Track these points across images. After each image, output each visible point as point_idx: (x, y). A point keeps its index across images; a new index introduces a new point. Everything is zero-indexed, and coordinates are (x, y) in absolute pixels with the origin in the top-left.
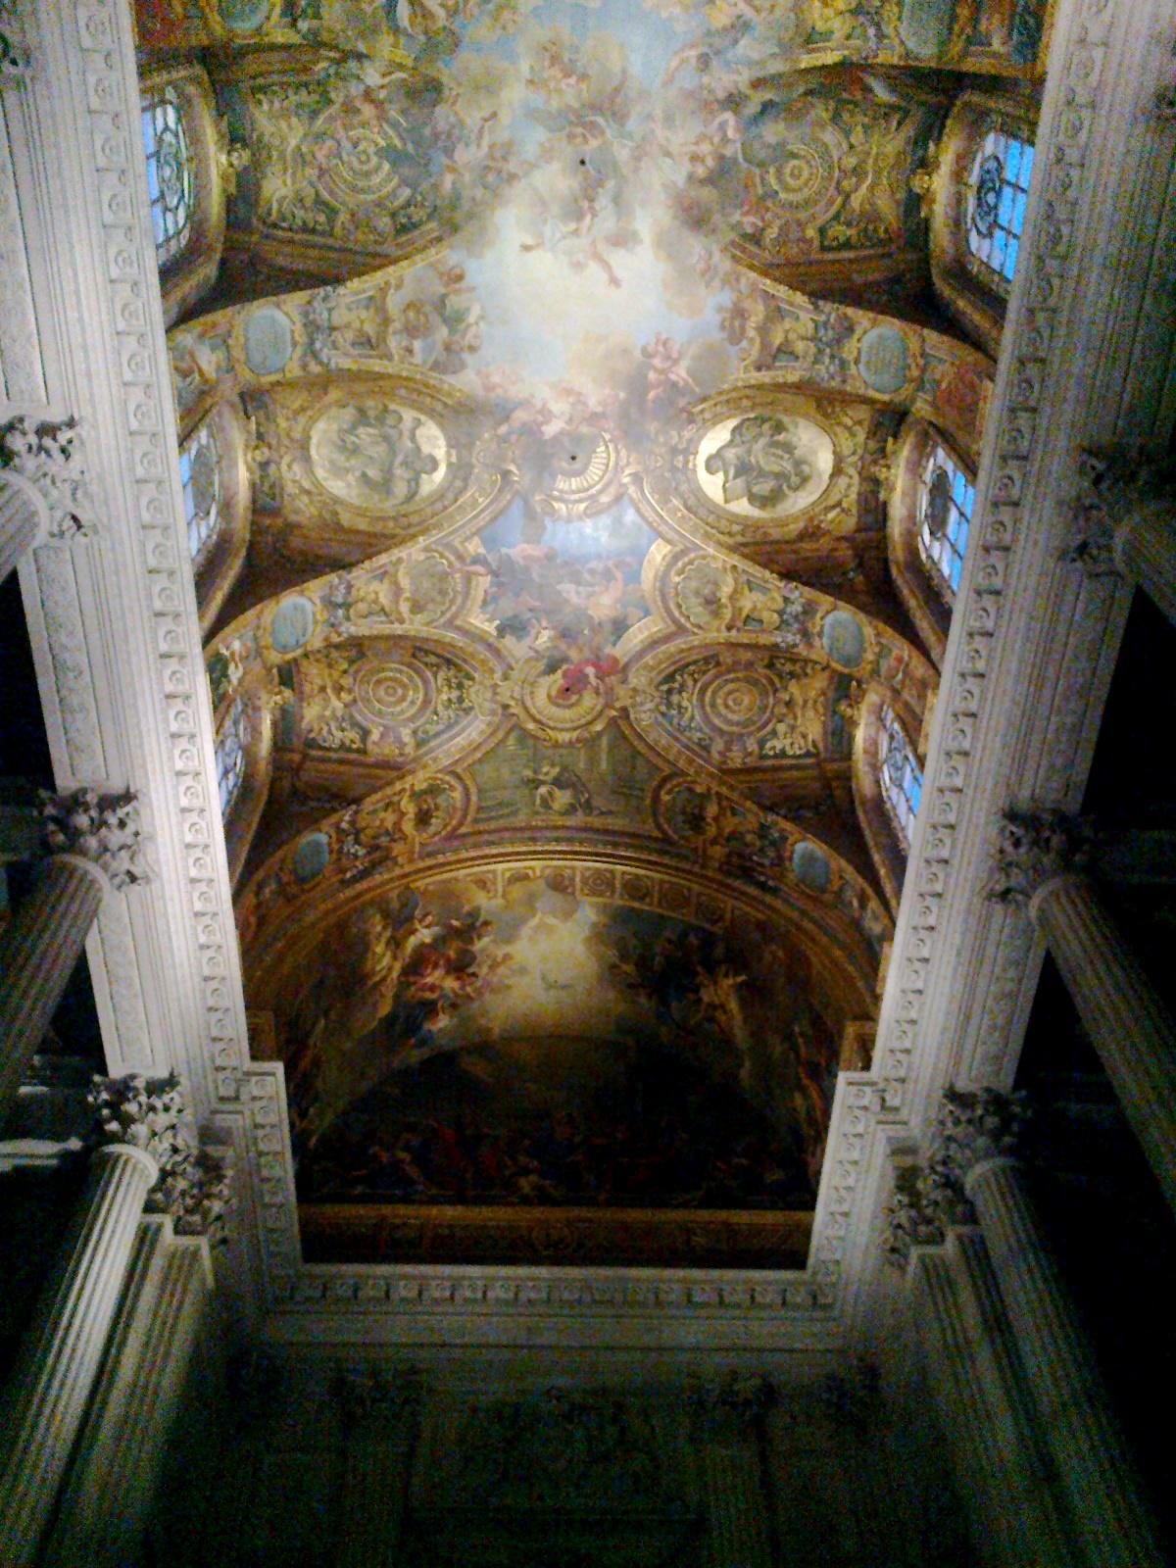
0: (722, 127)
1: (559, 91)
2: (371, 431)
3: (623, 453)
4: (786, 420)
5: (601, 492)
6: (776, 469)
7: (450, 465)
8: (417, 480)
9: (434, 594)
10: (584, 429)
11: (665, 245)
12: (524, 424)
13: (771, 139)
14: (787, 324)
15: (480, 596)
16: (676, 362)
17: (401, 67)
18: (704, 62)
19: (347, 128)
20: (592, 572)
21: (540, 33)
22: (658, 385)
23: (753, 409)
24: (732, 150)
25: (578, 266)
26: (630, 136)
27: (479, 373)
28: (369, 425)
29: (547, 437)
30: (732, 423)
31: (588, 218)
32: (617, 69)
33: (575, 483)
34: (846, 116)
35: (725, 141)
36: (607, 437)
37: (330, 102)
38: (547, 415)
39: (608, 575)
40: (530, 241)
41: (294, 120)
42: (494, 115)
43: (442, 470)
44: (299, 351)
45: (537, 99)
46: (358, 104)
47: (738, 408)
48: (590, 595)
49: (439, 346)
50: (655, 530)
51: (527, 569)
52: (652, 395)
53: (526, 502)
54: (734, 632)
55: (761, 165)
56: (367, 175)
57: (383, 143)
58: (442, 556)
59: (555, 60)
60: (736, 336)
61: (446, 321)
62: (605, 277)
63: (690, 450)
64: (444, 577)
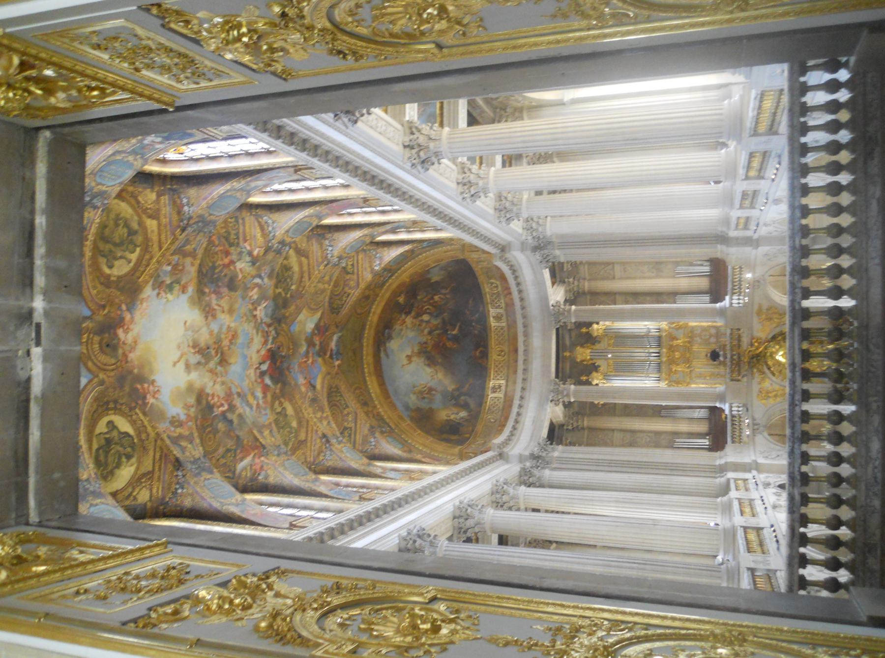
0: (222, 405)
2: (126, 235)
3: (112, 374)
4: (134, 460)
5: (92, 360)
6: (110, 459)
7: (109, 276)
8: (103, 256)
10: (120, 351)
11: (190, 388)
14: (190, 446)
16: (154, 397)
17: (245, 277)
18: (239, 394)
21: (239, 331)
22: (143, 388)
23: (141, 440)
24: (218, 411)
25: (179, 347)
27: (149, 296)
28: (129, 235)
30: (131, 431)
31: (193, 351)
32: (232, 360)
33: (96, 346)
35: (219, 407)
38: (126, 332)
40: (188, 324)
41: (224, 230)
43: (107, 271)
44: (207, 215)
46: (229, 258)
47: (140, 433)
49: (164, 279)
52: (139, 386)
57: (217, 264)
59: (233, 336)
61: (172, 283)
62: (176, 360)
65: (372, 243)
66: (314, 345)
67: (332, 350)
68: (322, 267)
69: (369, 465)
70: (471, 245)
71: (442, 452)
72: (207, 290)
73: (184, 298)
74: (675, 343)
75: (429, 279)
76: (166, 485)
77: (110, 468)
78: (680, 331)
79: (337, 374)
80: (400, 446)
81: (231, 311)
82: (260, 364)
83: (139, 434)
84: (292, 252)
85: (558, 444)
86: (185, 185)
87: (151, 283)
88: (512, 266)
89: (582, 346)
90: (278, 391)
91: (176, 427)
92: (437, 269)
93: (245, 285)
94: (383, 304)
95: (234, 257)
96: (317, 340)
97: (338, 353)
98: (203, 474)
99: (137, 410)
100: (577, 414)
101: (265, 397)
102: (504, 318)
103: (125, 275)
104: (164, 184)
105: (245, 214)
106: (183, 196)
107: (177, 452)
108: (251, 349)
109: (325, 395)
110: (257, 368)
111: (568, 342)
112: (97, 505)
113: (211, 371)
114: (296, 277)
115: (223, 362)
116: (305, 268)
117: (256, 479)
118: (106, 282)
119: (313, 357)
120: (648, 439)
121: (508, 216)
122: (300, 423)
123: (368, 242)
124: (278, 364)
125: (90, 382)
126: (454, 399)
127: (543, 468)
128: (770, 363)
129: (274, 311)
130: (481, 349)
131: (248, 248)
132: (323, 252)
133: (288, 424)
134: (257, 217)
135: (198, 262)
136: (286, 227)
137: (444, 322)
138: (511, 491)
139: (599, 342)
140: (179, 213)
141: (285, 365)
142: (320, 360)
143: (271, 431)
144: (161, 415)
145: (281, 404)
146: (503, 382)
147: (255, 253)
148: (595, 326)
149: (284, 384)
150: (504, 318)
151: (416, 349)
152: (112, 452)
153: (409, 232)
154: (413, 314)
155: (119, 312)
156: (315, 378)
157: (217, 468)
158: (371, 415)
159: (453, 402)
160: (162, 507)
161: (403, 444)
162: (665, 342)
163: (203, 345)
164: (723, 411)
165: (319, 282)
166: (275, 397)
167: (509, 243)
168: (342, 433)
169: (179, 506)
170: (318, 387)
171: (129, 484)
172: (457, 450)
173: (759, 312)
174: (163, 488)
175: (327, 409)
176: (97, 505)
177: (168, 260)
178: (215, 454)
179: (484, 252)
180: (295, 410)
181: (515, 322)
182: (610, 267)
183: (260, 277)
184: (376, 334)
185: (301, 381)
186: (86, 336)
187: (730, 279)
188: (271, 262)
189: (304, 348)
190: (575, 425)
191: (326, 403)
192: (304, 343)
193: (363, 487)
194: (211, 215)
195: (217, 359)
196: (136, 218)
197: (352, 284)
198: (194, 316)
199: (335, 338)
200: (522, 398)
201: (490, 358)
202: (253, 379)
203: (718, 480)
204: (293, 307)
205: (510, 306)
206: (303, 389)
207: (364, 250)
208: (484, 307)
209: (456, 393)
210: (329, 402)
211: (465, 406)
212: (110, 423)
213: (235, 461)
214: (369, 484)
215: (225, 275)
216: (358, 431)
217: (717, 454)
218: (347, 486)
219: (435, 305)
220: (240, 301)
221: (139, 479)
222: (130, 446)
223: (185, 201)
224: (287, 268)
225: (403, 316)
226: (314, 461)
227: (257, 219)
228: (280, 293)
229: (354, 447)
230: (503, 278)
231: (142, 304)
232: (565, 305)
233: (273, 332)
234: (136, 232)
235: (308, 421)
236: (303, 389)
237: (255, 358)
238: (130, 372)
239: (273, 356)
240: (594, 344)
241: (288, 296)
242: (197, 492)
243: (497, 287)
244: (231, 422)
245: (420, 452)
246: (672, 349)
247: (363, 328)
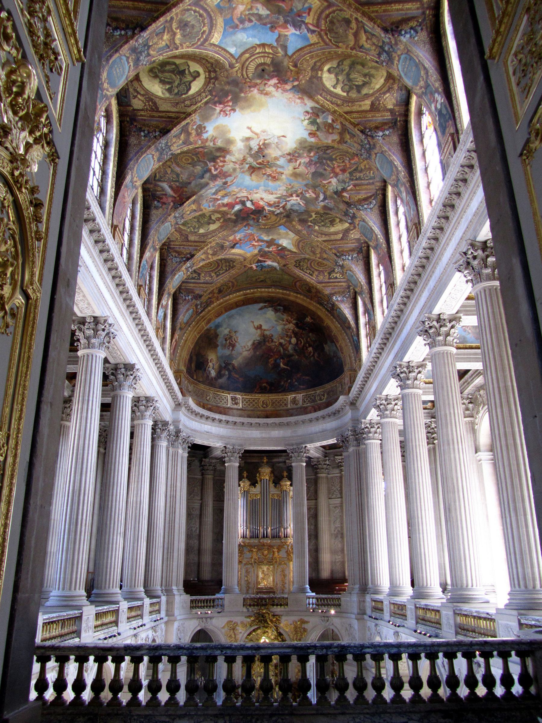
0: (216, 169)
1: (273, 172)
2: (357, 83)
3: (239, 75)
4: (167, 95)
6: (167, 74)
7: (322, 70)
8: (338, 65)
9: (337, 24)
10: (258, 81)
11: (230, 142)
12: (286, 83)
13: (199, 168)
14: (181, 142)
15: (312, 14)
16: (221, 111)
18: (226, 183)
19: (346, 165)
20: (250, 21)
21: (278, 183)
22: (228, 102)
23: (185, 100)
24: (210, 165)
25: (264, 132)
26: (247, 164)
27: (306, 104)
28: (356, 86)
29: (276, 79)
30: (191, 92)
34: (175, 176)
35: (214, 166)
36: (248, 80)
37: (350, 173)
38: (275, 86)
39: (242, 21)
41: (363, 168)
42: (294, 169)
43: (326, 68)
45: (279, 170)
46: (340, 173)
47: (190, 100)
48: (251, 9)
49: (321, 117)
50: (220, 47)
51: (286, 22)
52: (229, 98)
53: (286, 54)
54: (169, 18)
55: (200, 161)
56: (341, 155)
58: (330, 40)
59: (274, 177)
60: (200, 127)
61: (317, 124)
62: (253, 129)
63: (208, 81)
64: (331, 30)
65: (355, 293)
66: (268, 247)
67: (265, 261)
68: (334, 251)
69: (169, 294)
70: (355, 377)
71: (180, 356)
72: (312, 154)
73: (305, 135)
74: (275, 550)
75: (326, 343)
76: (147, 122)
77: (160, 75)
78: (285, 555)
79: (245, 266)
80: (185, 320)
81: (295, 175)
82: (251, 201)
83: (188, 99)
84: (347, 225)
85: (188, 453)
86: (400, 132)
87: (317, 106)
88: (339, 411)
89: (272, 472)
90: (229, 216)
91: (196, 130)
92: (335, 348)
93: (317, 187)
94: (305, 304)
95: (341, 177)
96: (272, 249)
97: (262, 267)
98: (158, 153)
99: (209, 97)
100: (215, 470)
101: (224, 205)
102: (295, 406)
103: (324, 85)
104: (400, 115)
105: (379, 184)
106: (391, 130)
107: (175, 131)
108: (263, 193)
109: (227, 257)
110: (248, 199)
111: (275, 460)
112: (128, 63)
113: (244, 160)
114: (325, 230)
115: (253, 170)
116: (333, 237)
117: (154, 199)
118: (317, 69)
119: (258, 245)
120: (194, 529)
121: (381, 407)
122: (203, 235)
123: (357, 290)
124: (252, 216)
125: (231, 55)
126: (225, 365)
127: (168, 439)
128: (259, 631)
129: (296, 211)
131: (349, 188)
132: (347, 251)
133: (201, 226)
134: (375, 195)
135: (336, 146)
136: (367, 219)
137: (290, 356)
138: (148, 413)
139: (275, 487)
140: (377, 128)
141: (251, 222)
142: (256, 251)
143: (195, 211)
144: (206, 118)
145: (218, 219)
146: (241, 406)
147: (345, 194)
148: (289, 483)
149: (235, 222)
151: (267, 333)
152: (174, 76)
153: (366, 325)
155: (291, 79)
156: (240, 248)
157: (163, 165)
158: (210, 296)
159: (223, 365)
160: (128, 119)
161: (187, 323)
162: (277, 541)
163: (266, 152)
164: (218, 593)
165: (322, 249)
166: (224, 214)
167: (358, 409)
168: (195, 271)
169: (130, 134)
170: (234, 251)
171: (147, 92)
172: (183, 368)
173: (303, 622)
174: (145, 120)
175: (215, 258)
176: (128, 63)
177: (337, 120)
178: (174, 165)
179: (350, 388)
180: (214, 231)
181: (292, 415)
182: (339, 496)
183: (325, 199)
184: (279, 299)
185: (238, 236)
186: (271, 51)
187: (330, 596)
188: (338, 207)
189: (265, 239)
190: (206, 467)
191: (220, 257)
192: (270, 238)
193: (150, 289)
194: (376, 154)
195: (254, 164)
196: (371, 92)
197: (321, 278)
198: (290, 144)
199: (275, 264)
200: (228, 422)
202: (239, 195)
203: (159, 588)
204: (299, 227)
205: (304, 411)
206: (231, 238)
207: (349, 287)
208: (304, 389)
209: (230, 367)
210: (221, 260)
211: (219, 375)
212: (198, 74)
213: (169, 181)
214: (152, 294)
215: (325, 170)
216: (197, 285)
217: (181, 587)
218: (151, 277)
219: (304, 348)
220: (305, 182)
221: (152, 100)
222: (179, 91)
223: (387, 133)
224: (332, 223)
225: (294, 322)
226: (170, 248)
227: (373, 195)
228: (311, 216)
229: (183, 282)
230: (329, 404)
231: (299, 98)
232: (306, 457)
233: (278, 211)
234: (359, 92)
235: (204, 242)
236: (231, 238)
237: (256, 197)
238: (241, 91)
239: (259, 211)
240: (273, 482)
241: (310, 224)
242: (142, 148)
243: (321, 399)
244: (202, 177)
245: (180, 337)
246: (270, 547)
247: (284, 288)
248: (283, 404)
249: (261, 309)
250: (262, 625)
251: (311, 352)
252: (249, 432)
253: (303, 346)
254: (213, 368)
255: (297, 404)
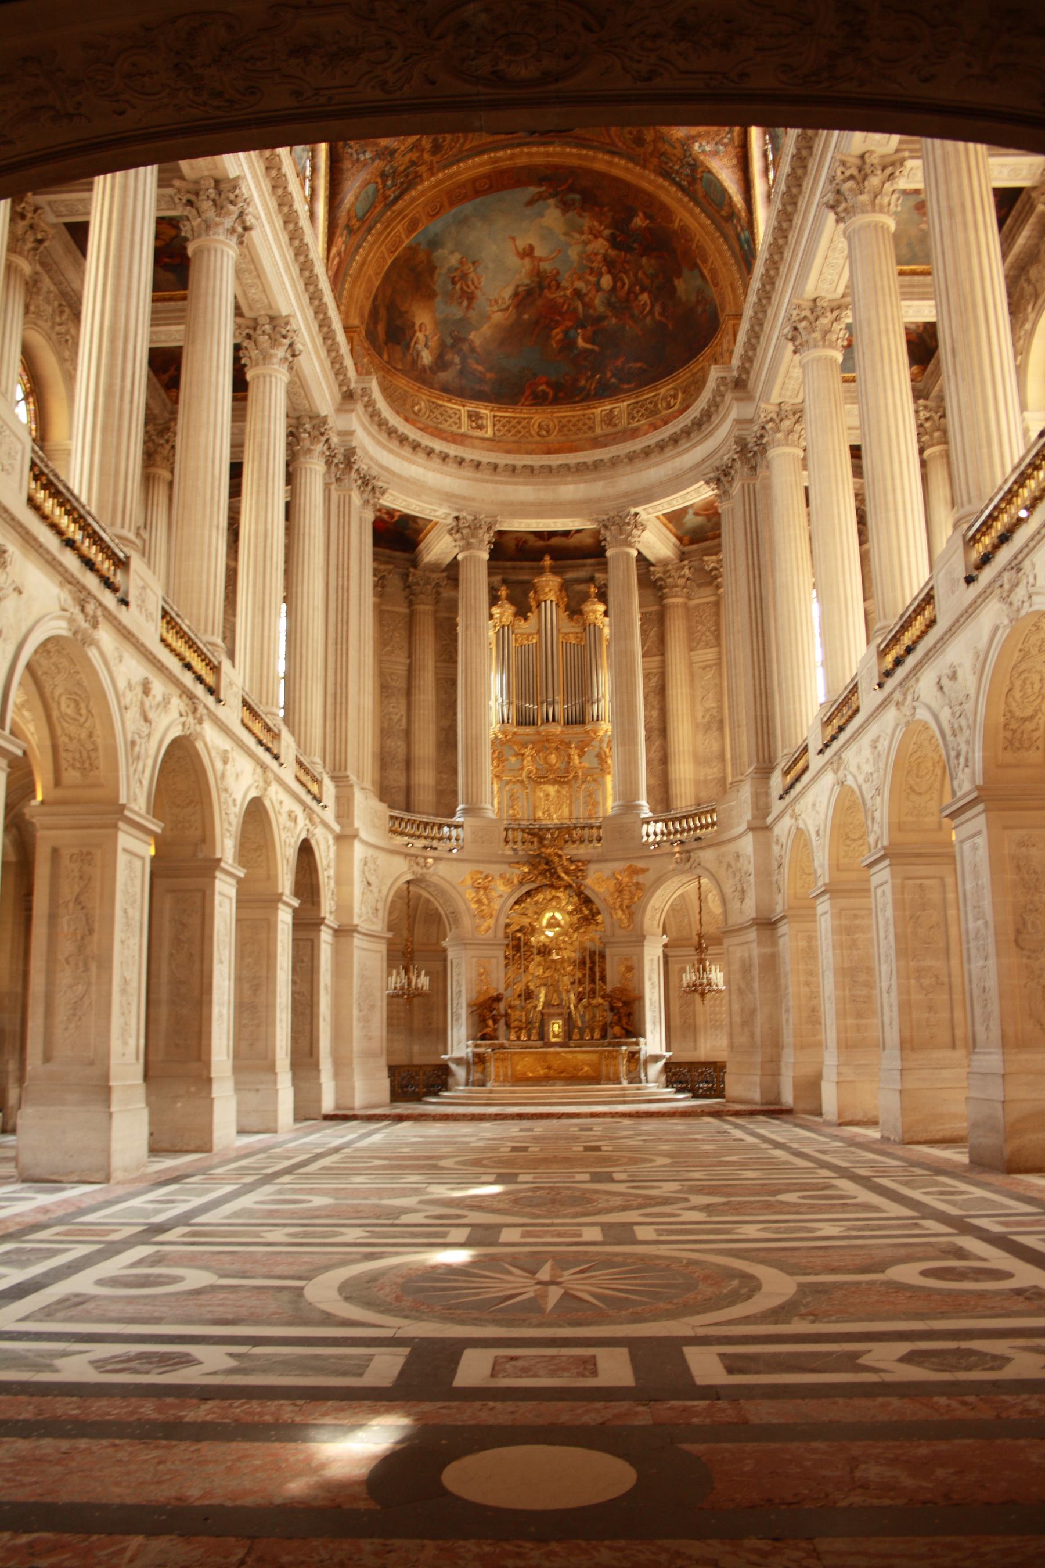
102: (610, 430)
126: (453, 339)
130: (551, 394)
146: (490, 433)
150: (610, 430)
154: (612, 253)
159: (449, 341)
201: (533, 409)
211: (441, 363)
248: (585, 428)
249: (530, 203)
250: (541, 881)
251: (645, 304)
252: (510, 488)
253: (629, 291)
254: (426, 346)
255: (616, 425)
